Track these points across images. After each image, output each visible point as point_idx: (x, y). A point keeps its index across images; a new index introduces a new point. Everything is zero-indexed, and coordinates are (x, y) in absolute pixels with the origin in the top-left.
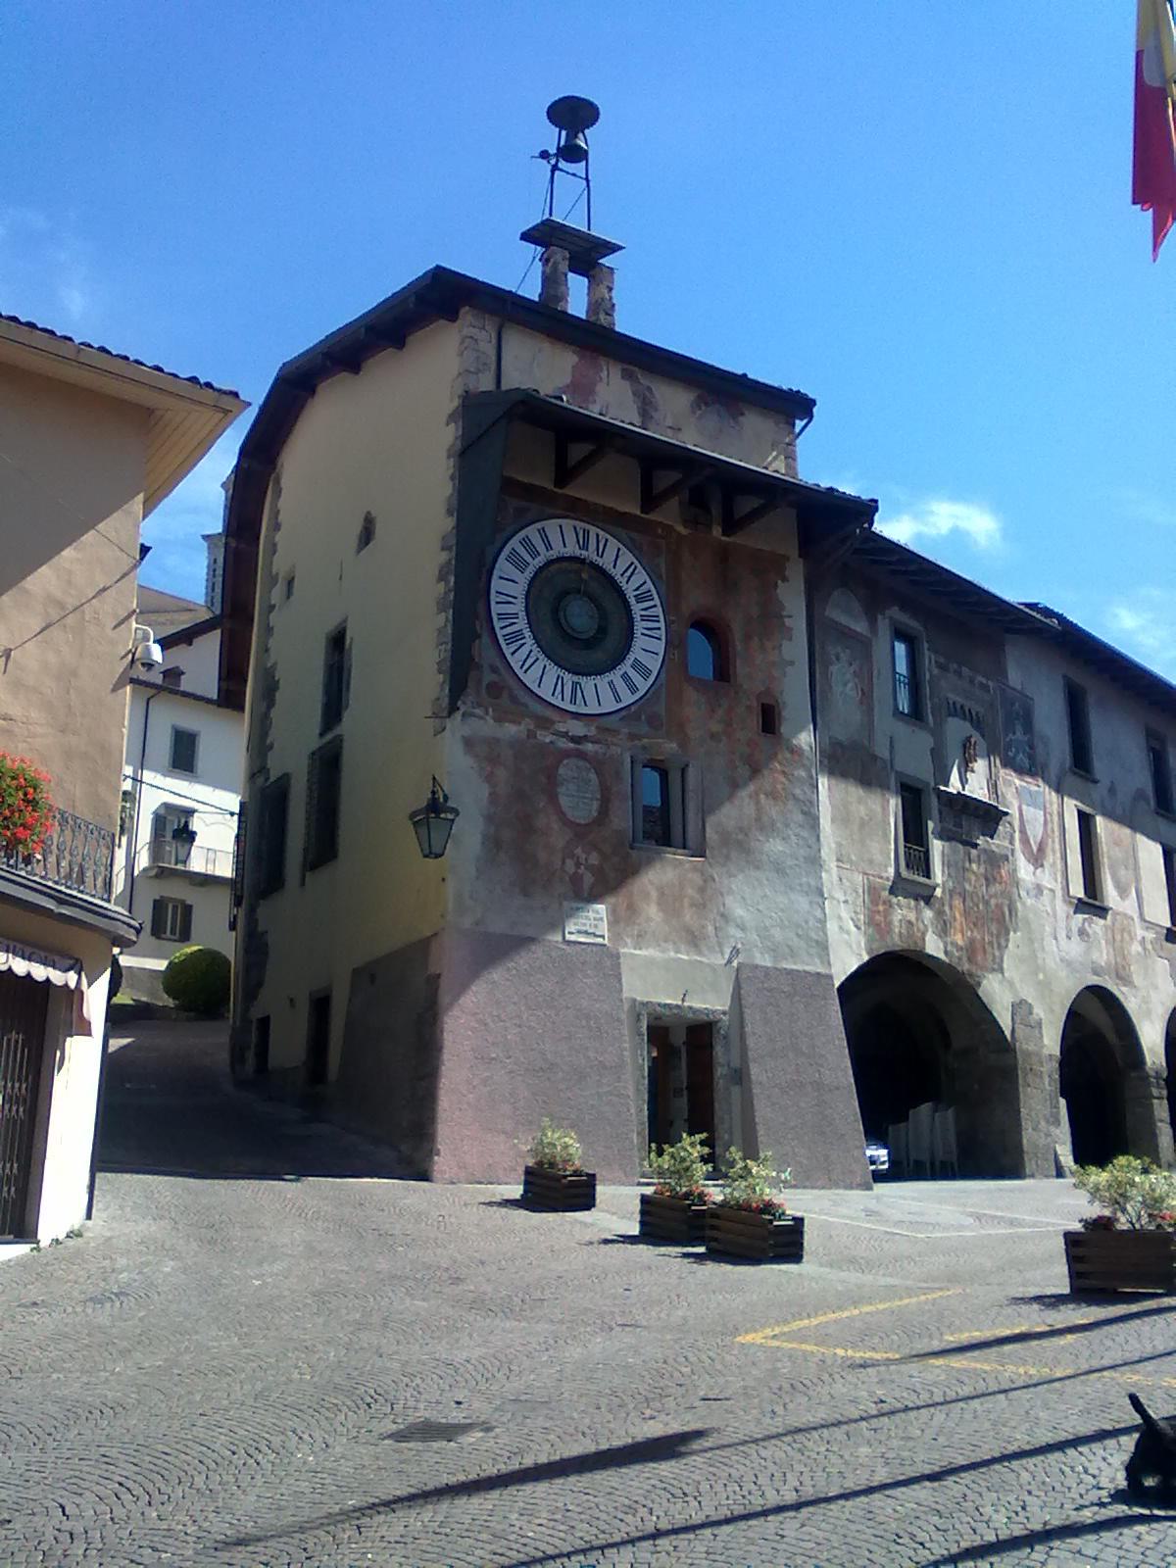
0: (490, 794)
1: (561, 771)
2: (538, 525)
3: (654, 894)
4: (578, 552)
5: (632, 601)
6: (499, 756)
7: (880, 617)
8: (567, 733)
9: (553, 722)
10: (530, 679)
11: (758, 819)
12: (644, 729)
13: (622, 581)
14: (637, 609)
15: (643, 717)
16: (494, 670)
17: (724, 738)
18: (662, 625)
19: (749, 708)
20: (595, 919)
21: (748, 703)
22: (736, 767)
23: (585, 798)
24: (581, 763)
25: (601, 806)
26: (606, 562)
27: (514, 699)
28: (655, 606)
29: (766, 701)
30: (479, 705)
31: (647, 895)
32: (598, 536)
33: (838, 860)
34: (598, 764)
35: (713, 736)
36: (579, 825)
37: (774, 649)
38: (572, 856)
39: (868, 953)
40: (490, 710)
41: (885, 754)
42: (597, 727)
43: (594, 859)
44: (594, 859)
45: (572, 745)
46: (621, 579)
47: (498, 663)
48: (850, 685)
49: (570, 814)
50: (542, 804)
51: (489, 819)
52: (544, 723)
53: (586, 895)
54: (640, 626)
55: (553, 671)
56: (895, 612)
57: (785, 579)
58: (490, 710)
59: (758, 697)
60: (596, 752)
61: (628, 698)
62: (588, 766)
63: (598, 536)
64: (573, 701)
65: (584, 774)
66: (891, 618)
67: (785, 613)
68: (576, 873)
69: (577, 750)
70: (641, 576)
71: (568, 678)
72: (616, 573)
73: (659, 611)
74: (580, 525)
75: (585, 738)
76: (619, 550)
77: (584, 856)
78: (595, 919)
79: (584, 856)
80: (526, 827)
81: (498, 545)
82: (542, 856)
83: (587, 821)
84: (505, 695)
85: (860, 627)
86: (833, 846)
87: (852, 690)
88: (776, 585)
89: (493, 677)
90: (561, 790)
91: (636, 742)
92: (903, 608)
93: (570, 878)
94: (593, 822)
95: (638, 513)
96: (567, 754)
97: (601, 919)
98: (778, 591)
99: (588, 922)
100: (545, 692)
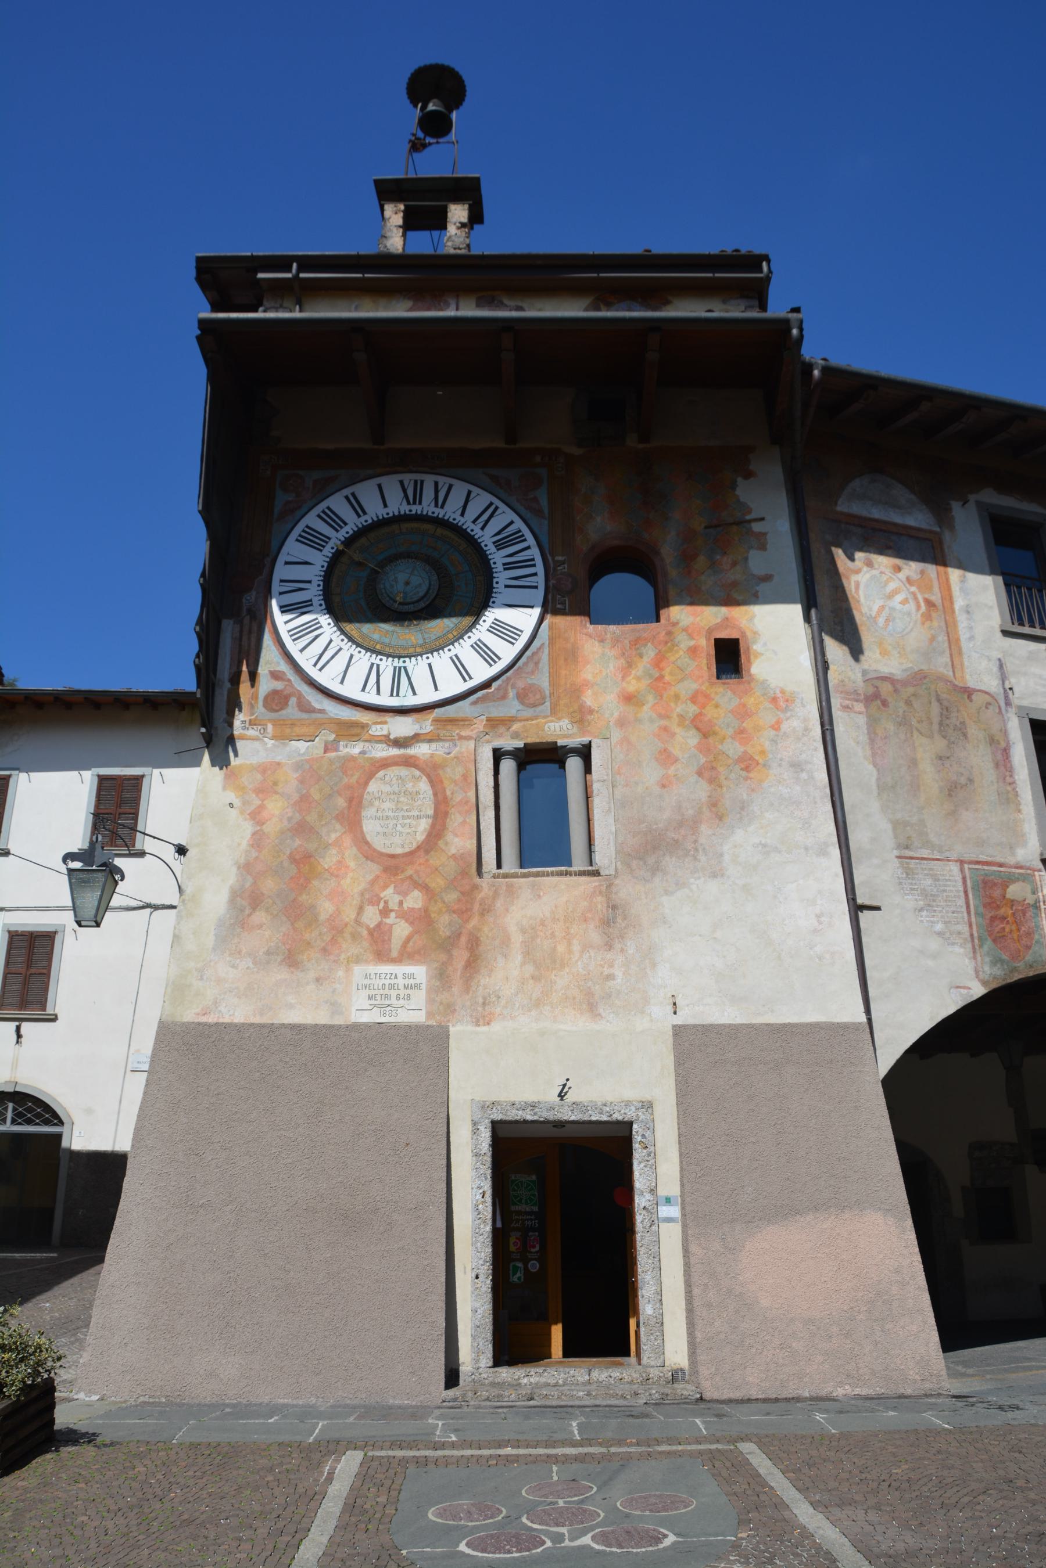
0: (254, 834)
1: (373, 787)
2: (347, 491)
3: (517, 939)
4: (405, 508)
5: (491, 549)
6: (275, 784)
7: (956, 506)
8: (387, 736)
9: (364, 727)
10: (327, 678)
11: (714, 804)
12: (512, 707)
13: (476, 531)
14: (498, 558)
15: (511, 694)
16: (276, 675)
17: (651, 699)
18: (540, 568)
19: (693, 651)
20: (406, 987)
21: (692, 643)
22: (674, 735)
23: (409, 817)
24: (403, 771)
25: (433, 826)
26: (451, 511)
27: (305, 707)
28: (528, 548)
29: (723, 635)
30: (252, 723)
31: (506, 941)
32: (436, 484)
33: (899, 847)
34: (432, 771)
35: (629, 699)
36: (393, 856)
37: (734, 564)
38: (375, 900)
39: (984, 983)
40: (270, 727)
41: (991, 683)
42: (436, 721)
43: (415, 900)
44: (415, 900)
45: (395, 751)
46: (472, 526)
47: (283, 667)
48: (899, 598)
49: (380, 844)
50: (334, 836)
51: (246, 868)
52: (350, 731)
53: (394, 954)
54: (501, 577)
55: (364, 660)
56: (991, 497)
57: (748, 475)
58: (270, 727)
59: (710, 631)
60: (432, 756)
61: (481, 672)
62: (417, 773)
63: (436, 484)
64: (395, 691)
65: (409, 786)
66: (979, 505)
67: (748, 517)
68: (379, 925)
69: (404, 755)
70: (505, 516)
71: (388, 666)
72: (466, 522)
73: (535, 552)
74: (408, 478)
75: (416, 738)
76: (469, 493)
77: (397, 898)
78: (406, 987)
79: (397, 898)
80: (304, 866)
81: (290, 526)
82: (326, 908)
83: (407, 850)
84: (293, 701)
85: (918, 519)
86: (889, 826)
87: (904, 602)
88: (733, 486)
89: (279, 685)
90: (368, 813)
91: (502, 729)
92: (1003, 486)
93: (371, 932)
94: (419, 848)
95: (502, 445)
96: (385, 764)
97: (417, 986)
98: (738, 492)
99: (394, 993)
100: (351, 690)
